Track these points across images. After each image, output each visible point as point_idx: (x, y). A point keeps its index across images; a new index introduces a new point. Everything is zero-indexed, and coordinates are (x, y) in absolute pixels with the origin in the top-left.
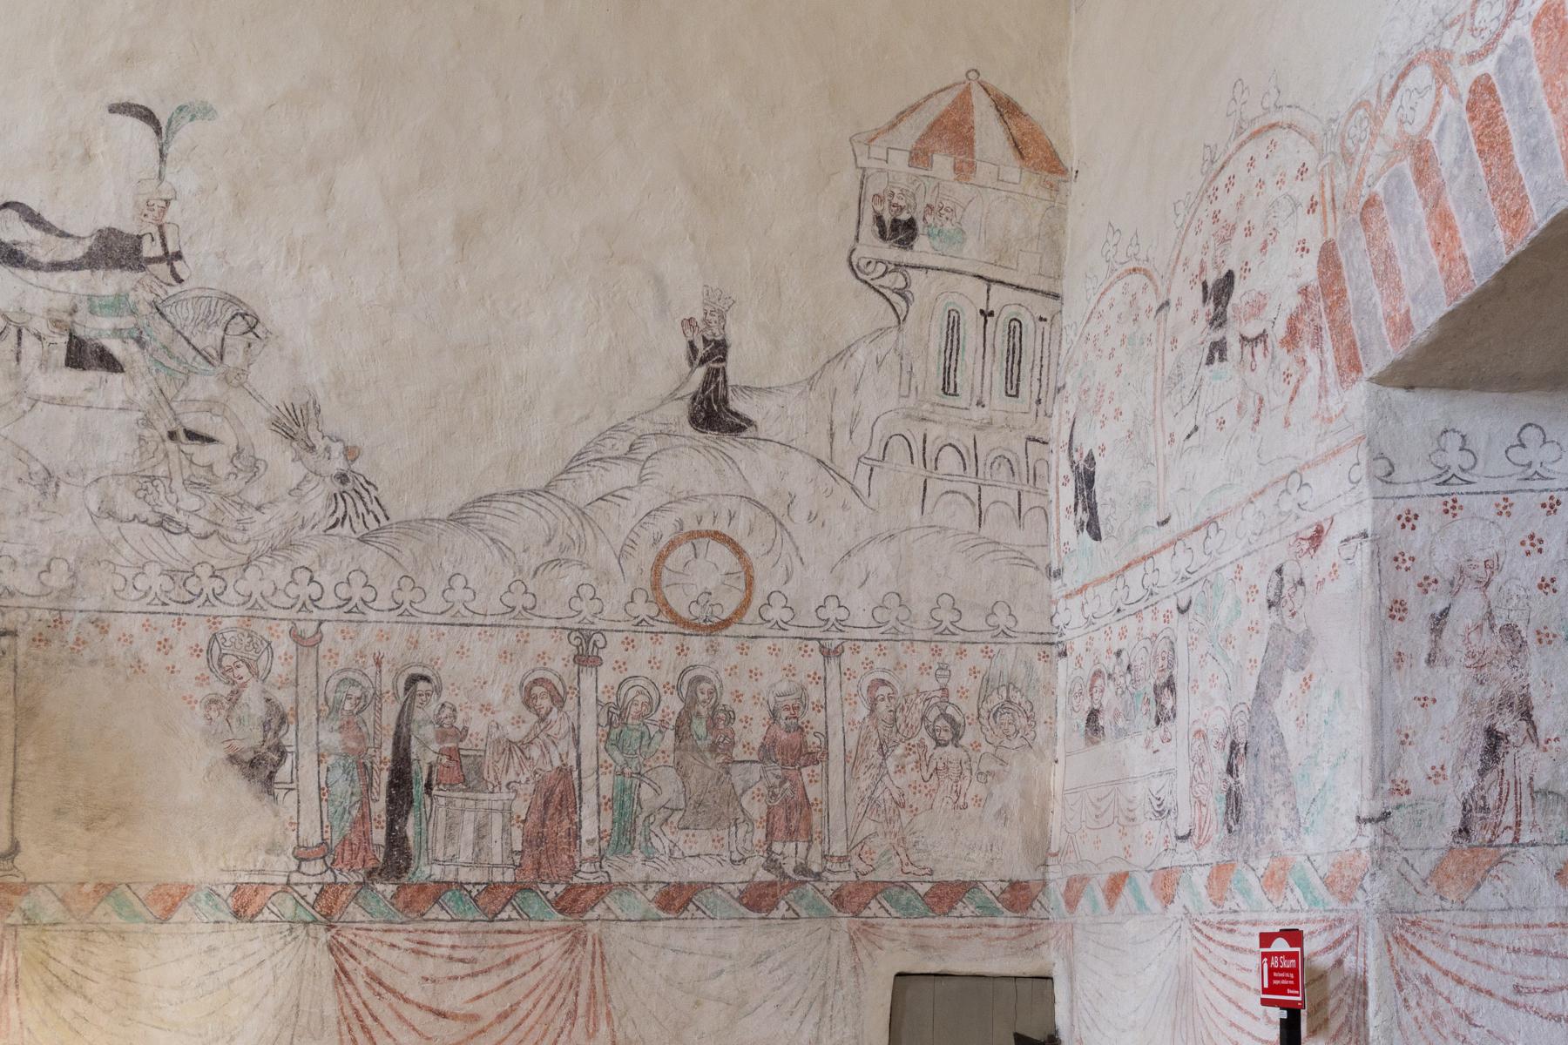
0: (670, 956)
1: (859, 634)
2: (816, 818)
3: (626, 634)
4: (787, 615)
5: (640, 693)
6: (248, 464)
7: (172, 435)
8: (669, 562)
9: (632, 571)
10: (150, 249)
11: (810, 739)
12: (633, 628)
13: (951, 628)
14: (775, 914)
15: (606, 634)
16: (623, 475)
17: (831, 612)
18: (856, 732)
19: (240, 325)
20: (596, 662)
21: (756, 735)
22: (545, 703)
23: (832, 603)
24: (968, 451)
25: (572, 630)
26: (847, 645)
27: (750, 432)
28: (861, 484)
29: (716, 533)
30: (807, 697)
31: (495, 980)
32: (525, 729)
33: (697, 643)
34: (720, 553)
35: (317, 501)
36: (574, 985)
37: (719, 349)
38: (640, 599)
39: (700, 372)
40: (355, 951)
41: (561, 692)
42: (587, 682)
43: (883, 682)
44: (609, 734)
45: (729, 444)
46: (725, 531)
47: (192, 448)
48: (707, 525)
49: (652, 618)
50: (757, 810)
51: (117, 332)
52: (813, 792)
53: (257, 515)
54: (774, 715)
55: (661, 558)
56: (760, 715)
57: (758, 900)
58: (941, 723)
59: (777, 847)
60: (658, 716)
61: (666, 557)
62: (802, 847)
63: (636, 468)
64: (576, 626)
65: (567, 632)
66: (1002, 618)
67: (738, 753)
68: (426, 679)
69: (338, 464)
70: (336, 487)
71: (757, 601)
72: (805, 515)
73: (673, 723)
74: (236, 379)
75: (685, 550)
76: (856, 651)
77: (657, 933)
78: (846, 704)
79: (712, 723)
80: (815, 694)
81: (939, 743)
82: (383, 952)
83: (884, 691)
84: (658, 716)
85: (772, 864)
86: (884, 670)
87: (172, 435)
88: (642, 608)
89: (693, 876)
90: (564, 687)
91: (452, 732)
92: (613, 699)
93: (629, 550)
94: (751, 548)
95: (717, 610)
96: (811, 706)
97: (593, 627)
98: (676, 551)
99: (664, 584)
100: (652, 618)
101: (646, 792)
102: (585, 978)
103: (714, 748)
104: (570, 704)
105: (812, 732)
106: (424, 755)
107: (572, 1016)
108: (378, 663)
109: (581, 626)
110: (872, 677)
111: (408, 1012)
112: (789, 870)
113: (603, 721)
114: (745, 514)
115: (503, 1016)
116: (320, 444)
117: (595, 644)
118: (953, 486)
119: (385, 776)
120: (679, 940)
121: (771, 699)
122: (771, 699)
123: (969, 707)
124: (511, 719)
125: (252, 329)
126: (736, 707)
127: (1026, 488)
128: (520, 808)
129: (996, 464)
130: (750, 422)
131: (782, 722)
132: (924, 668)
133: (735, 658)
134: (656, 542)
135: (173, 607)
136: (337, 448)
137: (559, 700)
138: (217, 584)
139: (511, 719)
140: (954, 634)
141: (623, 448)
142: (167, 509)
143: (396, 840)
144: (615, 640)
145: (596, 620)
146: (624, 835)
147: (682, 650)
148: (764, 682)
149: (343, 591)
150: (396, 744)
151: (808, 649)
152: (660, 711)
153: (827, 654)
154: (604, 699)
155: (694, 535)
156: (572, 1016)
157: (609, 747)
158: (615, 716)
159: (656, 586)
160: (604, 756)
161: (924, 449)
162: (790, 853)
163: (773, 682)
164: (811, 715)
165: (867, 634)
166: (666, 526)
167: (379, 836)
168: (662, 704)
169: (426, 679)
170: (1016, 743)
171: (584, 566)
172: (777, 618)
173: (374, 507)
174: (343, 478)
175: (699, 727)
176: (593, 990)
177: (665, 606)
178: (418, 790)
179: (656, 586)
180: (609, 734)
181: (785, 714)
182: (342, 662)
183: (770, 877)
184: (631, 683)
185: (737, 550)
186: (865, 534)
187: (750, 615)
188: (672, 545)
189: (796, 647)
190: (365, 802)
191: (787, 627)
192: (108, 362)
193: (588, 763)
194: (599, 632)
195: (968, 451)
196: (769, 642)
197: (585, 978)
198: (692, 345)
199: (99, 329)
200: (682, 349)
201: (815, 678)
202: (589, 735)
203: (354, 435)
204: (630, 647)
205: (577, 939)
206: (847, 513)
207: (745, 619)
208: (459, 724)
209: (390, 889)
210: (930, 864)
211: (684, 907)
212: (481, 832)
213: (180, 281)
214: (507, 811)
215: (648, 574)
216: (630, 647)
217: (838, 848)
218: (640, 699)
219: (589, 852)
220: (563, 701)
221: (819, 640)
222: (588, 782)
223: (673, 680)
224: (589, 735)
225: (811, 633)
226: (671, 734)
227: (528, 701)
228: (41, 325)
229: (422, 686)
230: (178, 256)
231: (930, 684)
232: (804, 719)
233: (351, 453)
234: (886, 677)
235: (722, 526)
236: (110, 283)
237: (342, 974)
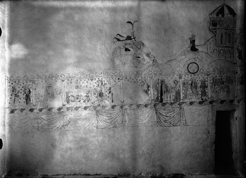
0: (191, 110)
2: (207, 94)
4: (203, 71)
6: (144, 59)
7: (136, 57)
9: (185, 67)
10: (132, 37)
11: (206, 85)
14: (203, 104)
16: (183, 57)
17: (208, 70)
19: (142, 45)
20: (182, 78)
21: (200, 85)
22: (176, 83)
23: (208, 69)
27: (198, 50)
28: (211, 55)
31: (172, 113)
32: (174, 86)
33: (193, 75)
34: (196, 65)
35: (151, 62)
36: (181, 112)
37: (194, 41)
38: (186, 71)
39: (192, 44)
40: (158, 110)
42: (181, 80)
43: (214, 78)
45: (196, 53)
47: (138, 58)
48: (193, 62)
50: (200, 93)
51: (130, 47)
52: (206, 91)
53: (145, 65)
54: (202, 83)
55: (188, 66)
56: (200, 83)
57: (200, 103)
59: (202, 97)
60: (189, 84)
62: (205, 97)
63: (185, 56)
66: (229, 69)
67: (198, 87)
68: (164, 81)
69: (153, 59)
70: (153, 61)
71: (199, 70)
72: (204, 59)
74: (142, 51)
75: (191, 65)
76: (211, 75)
77: (189, 107)
79: (195, 84)
80: (206, 80)
81: (221, 85)
82: (161, 110)
83: (214, 79)
84: (189, 84)
85: (202, 99)
87: (136, 57)
88: (186, 72)
89: (193, 101)
91: (166, 87)
94: (198, 64)
101: (188, 92)
102: (182, 112)
103: (195, 87)
104: (179, 83)
106: (164, 89)
107: (181, 116)
108: (158, 80)
111: (164, 116)
112: (204, 99)
113: (183, 84)
114: (197, 60)
115: (173, 117)
116: (151, 57)
119: (160, 92)
120: (192, 108)
123: (225, 80)
124: (173, 85)
125: (143, 45)
128: (174, 94)
130: (198, 50)
132: (219, 76)
133: (197, 76)
134: (188, 64)
135: (137, 76)
136: (153, 57)
137: (178, 82)
138: (141, 73)
139: (173, 85)
141: (183, 54)
142: (136, 65)
143: (161, 98)
146: (185, 97)
147: (191, 76)
148: (200, 79)
149: (154, 72)
150: (161, 89)
154: (183, 82)
156: (181, 116)
158: (184, 84)
160: (183, 88)
162: (204, 98)
163: (201, 78)
165: (212, 73)
167: (160, 98)
169: (164, 81)
170: (231, 84)
171: (180, 67)
173: (157, 63)
174: (153, 60)
175: (193, 84)
176: (183, 114)
177: (189, 71)
178: (163, 93)
179: (188, 69)
182: (155, 80)
183: (202, 101)
186: (212, 61)
187: (199, 71)
190: (158, 95)
192: (129, 50)
193: (181, 89)
197: (182, 112)
198: (191, 41)
199: (127, 47)
200: (189, 42)
201: (206, 78)
202: (181, 86)
203: (155, 56)
205: (181, 108)
208: (167, 86)
209: (161, 104)
210: (220, 98)
211: (192, 104)
212: (170, 98)
213: (135, 40)
214: (173, 95)
215: (187, 68)
217: (210, 97)
219: (182, 99)
222: (181, 91)
224: (181, 86)
225: (206, 73)
226: (190, 85)
227: (175, 83)
228: (122, 47)
229: (163, 82)
230: (135, 38)
231: (220, 78)
233: (154, 57)
235: (195, 62)
236: (129, 41)
237: (156, 113)
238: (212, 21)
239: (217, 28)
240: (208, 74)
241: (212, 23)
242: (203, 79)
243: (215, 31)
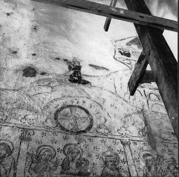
1: (135, 139)
3: (43, 131)
4: (106, 131)
5: (47, 151)
8: (62, 112)
12: (46, 130)
13: (169, 139)
15: (34, 130)
18: (142, 172)
20: (29, 139)
25: (20, 128)
26: (131, 142)
29: (79, 106)
30: (119, 158)
41: (12, 149)
43: (148, 155)
44: (31, 165)
46: (83, 106)
49: (54, 128)
54: (106, 163)
55: (58, 111)
56: (99, 163)
58: (175, 171)
61: (60, 111)
64: (22, 127)
65: (18, 128)
71: (95, 126)
73: (61, 163)
78: (135, 161)
79: (78, 165)
80: (122, 157)
84: (55, 160)
86: (148, 151)
88: (50, 124)
90: (13, 147)
92: (35, 153)
93: (46, 108)
95: (79, 127)
96: (121, 161)
97: (29, 128)
98: (64, 110)
99: (59, 118)
100: (54, 128)
104: (15, 153)
105: (123, 171)
109: (24, 127)
110: (144, 153)
117: (29, 134)
121: (104, 157)
122: (104, 157)
126: (89, 159)
131: (110, 166)
140: (170, 141)
144: (38, 134)
145: (31, 126)
147: (65, 138)
151: (117, 142)
152: (55, 158)
153: (124, 144)
154: (31, 153)
155: (70, 106)
157: (31, 171)
159: (56, 118)
164: (121, 164)
165: (138, 139)
166: (60, 103)
168: (56, 155)
172: (103, 132)
180: (31, 165)
181: (110, 163)
184: (44, 147)
185: (87, 112)
188: (62, 108)
189: (112, 142)
191: (107, 135)
194: (30, 130)
196: (101, 139)
204: (44, 136)
206: (123, 106)
207: (91, 131)
216: (44, 136)
218: (46, 153)
220: (12, 152)
221: (120, 140)
223: (61, 148)
225: (116, 137)
232: (119, 166)
234: (150, 153)
235: (81, 104)
240: (126, 139)
242: (109, 153)
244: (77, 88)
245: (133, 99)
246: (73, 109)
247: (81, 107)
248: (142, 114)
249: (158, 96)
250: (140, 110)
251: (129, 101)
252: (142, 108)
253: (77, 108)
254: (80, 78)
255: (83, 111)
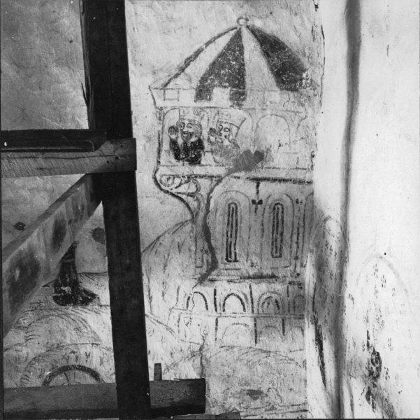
24: (246, 298)
29: (80, 366)
46: (84, 364)
118: (235, 321)
127: (287, 316)
129: (266, 304)
161: (215, 299)
195: (246, 298)
238: (173, 129)
239: (197, 170)
241: (173, 143)
243: (193, 189)
244: (72, 317)
245: (187, 320)
246: (71, 373)
247: (84, 367)
248: (199, 359)
249: (244, 301)
250: (197, 348)
251: (175, 329)
252: (201, 342)
253: (77, 372)
254: (75, 284)
255: (87, 376)
